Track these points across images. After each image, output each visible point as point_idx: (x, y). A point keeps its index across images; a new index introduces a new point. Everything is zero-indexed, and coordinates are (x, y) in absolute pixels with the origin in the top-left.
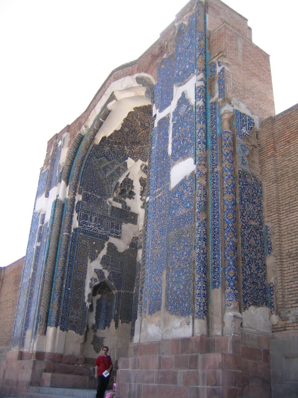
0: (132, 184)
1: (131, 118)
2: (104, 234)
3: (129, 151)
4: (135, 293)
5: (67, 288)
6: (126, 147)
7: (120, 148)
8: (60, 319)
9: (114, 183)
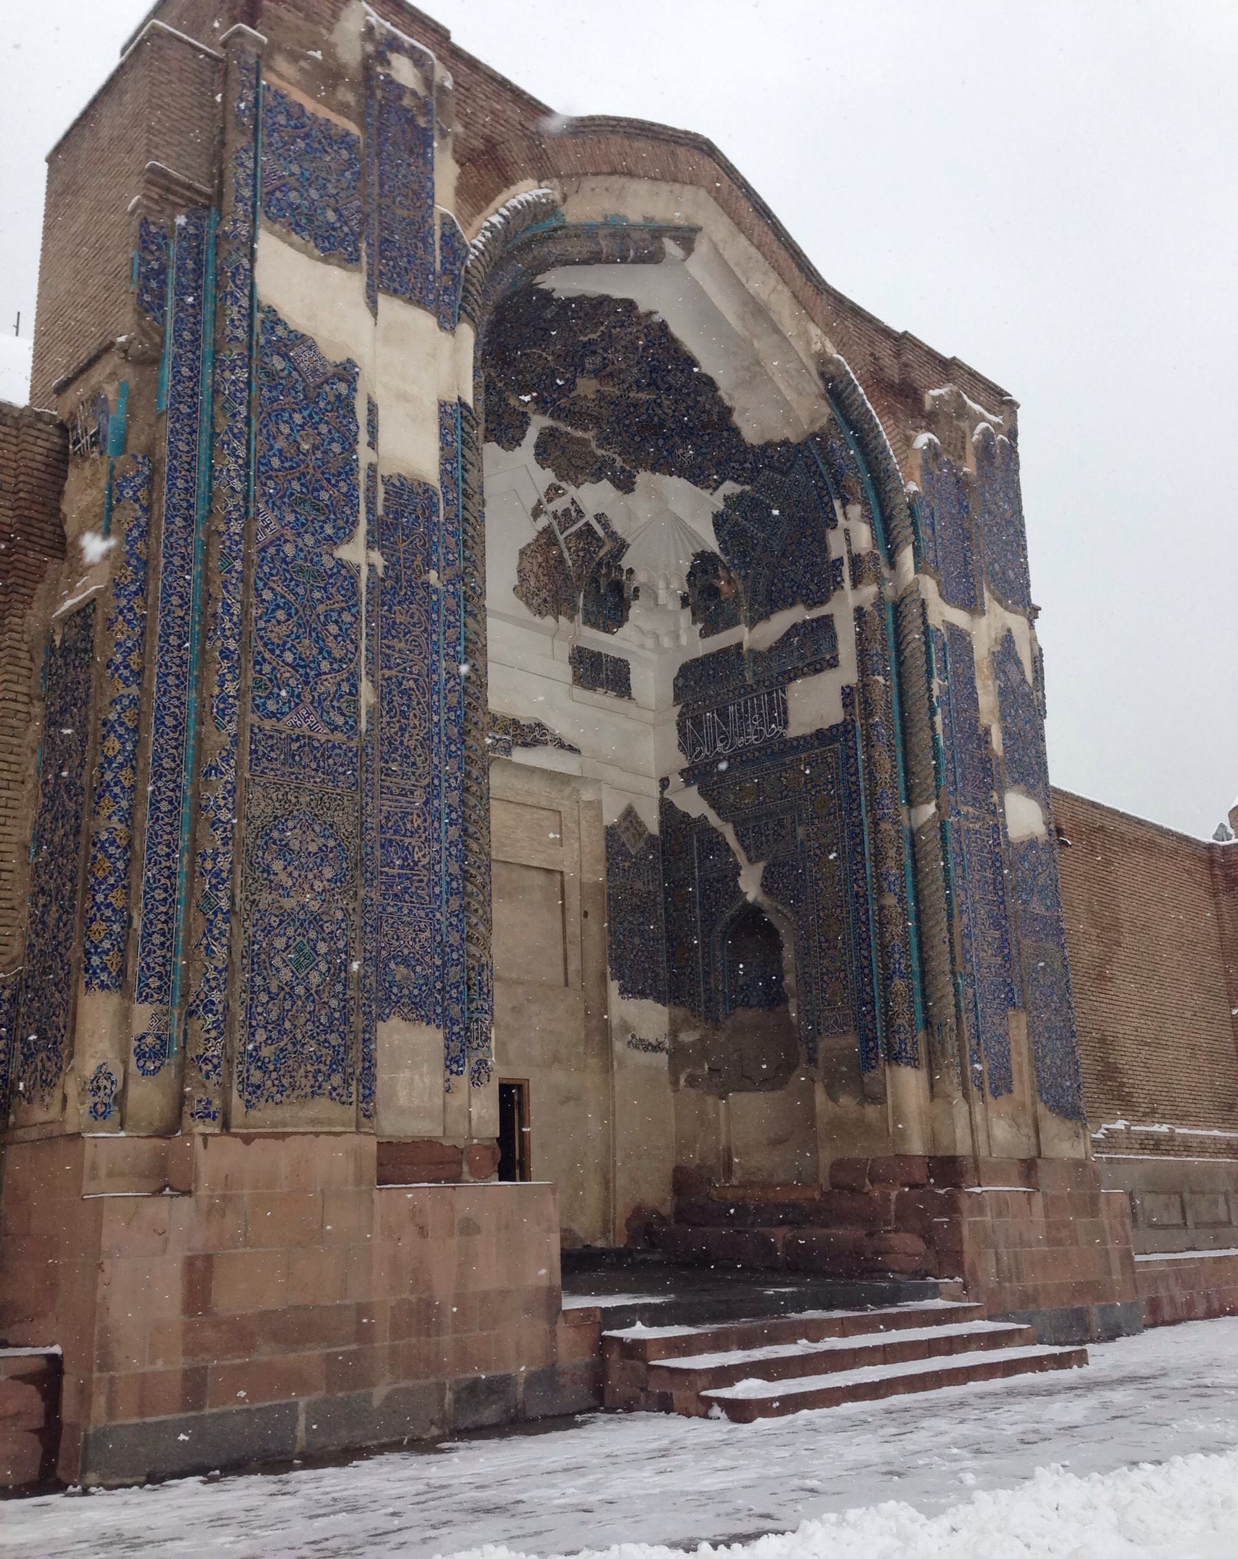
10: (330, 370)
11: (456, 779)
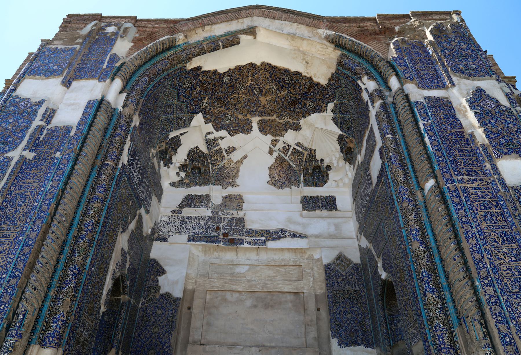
0: (177, 148)
1: (245, 71)
2: (140, 196)
3: (206, 105)
4: (141, 308)
5: (91, 267)
6: (207, 98)
7: (200, 95)
8: (68, 331)
9: (164, 132)
10: (33, 104)
11: (38, 227)
